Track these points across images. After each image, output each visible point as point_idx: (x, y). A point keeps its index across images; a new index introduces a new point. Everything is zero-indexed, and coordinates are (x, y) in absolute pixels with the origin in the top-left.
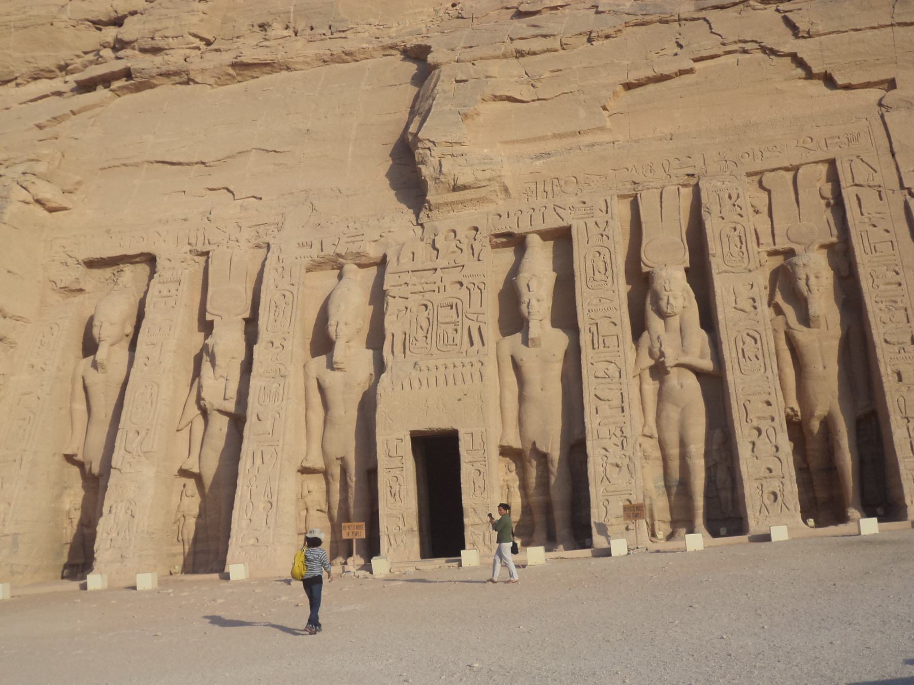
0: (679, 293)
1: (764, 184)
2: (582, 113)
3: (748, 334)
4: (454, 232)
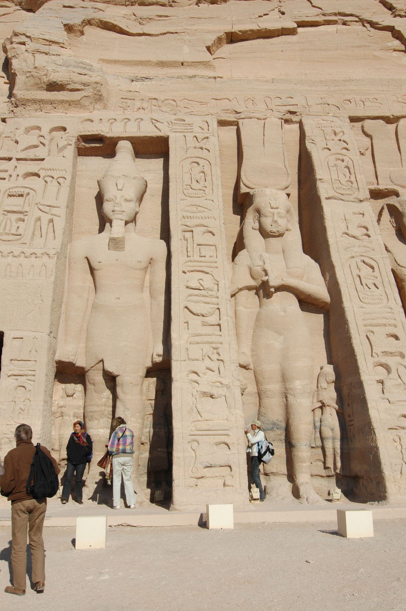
0: (282, 211)
1: (366, 129)
2: (186, 49)
3: (364, 262)
4: (39, 128)
